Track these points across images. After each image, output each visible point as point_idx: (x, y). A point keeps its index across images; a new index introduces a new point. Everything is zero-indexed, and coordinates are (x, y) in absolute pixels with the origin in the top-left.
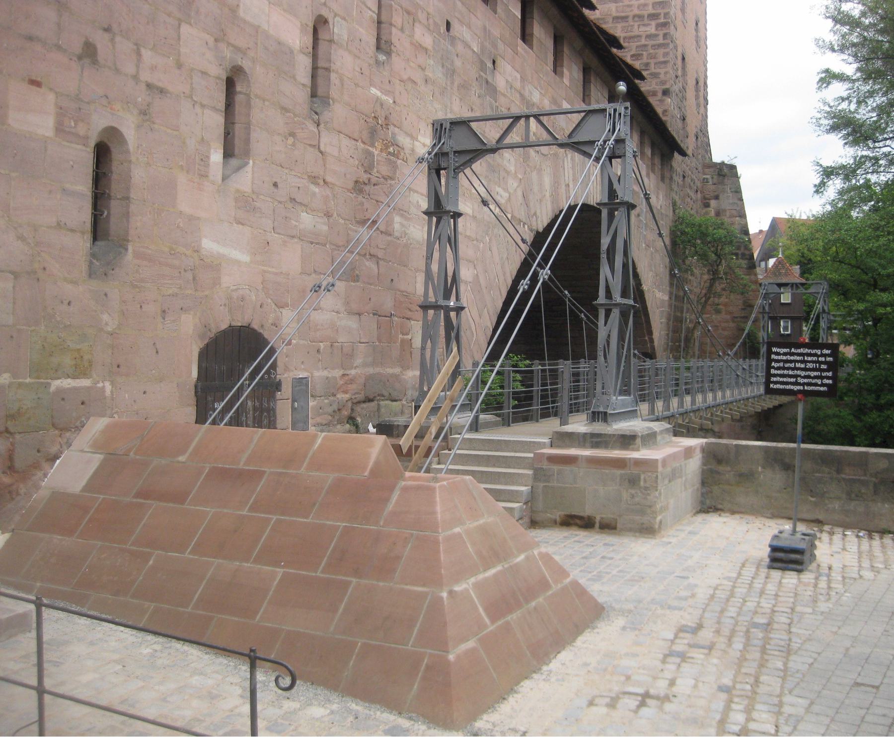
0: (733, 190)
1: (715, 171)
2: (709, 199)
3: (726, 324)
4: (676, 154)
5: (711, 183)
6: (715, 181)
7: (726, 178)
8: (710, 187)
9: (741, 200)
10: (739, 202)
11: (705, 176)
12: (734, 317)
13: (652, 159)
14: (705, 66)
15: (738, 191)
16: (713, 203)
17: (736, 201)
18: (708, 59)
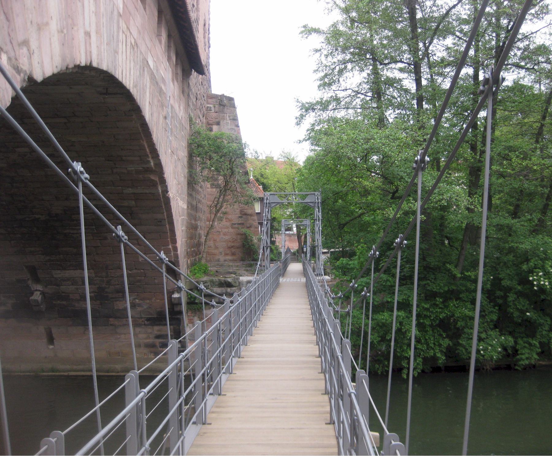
0: (231, 118)
1: (216, 102)
2: (212, 125)
3: (226, 230)
4: (194, 74)
5: (213, 111)
6: (217, 109)
7: (226, 107)
8: (213, 114)
9: (238, 126)
10: (236, 128)
11: (208, 105)
12: (233, 224)
13: (177, 64)
14: (209, 15)
15: (235, 119)
16: (215, 128)
17: (234, 127)
18: (211, 10)
